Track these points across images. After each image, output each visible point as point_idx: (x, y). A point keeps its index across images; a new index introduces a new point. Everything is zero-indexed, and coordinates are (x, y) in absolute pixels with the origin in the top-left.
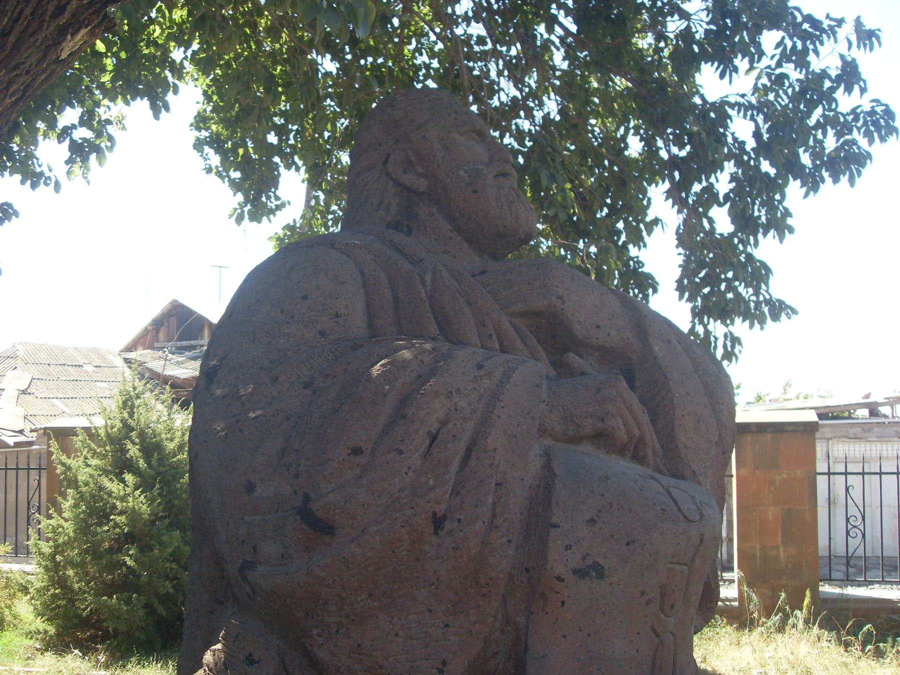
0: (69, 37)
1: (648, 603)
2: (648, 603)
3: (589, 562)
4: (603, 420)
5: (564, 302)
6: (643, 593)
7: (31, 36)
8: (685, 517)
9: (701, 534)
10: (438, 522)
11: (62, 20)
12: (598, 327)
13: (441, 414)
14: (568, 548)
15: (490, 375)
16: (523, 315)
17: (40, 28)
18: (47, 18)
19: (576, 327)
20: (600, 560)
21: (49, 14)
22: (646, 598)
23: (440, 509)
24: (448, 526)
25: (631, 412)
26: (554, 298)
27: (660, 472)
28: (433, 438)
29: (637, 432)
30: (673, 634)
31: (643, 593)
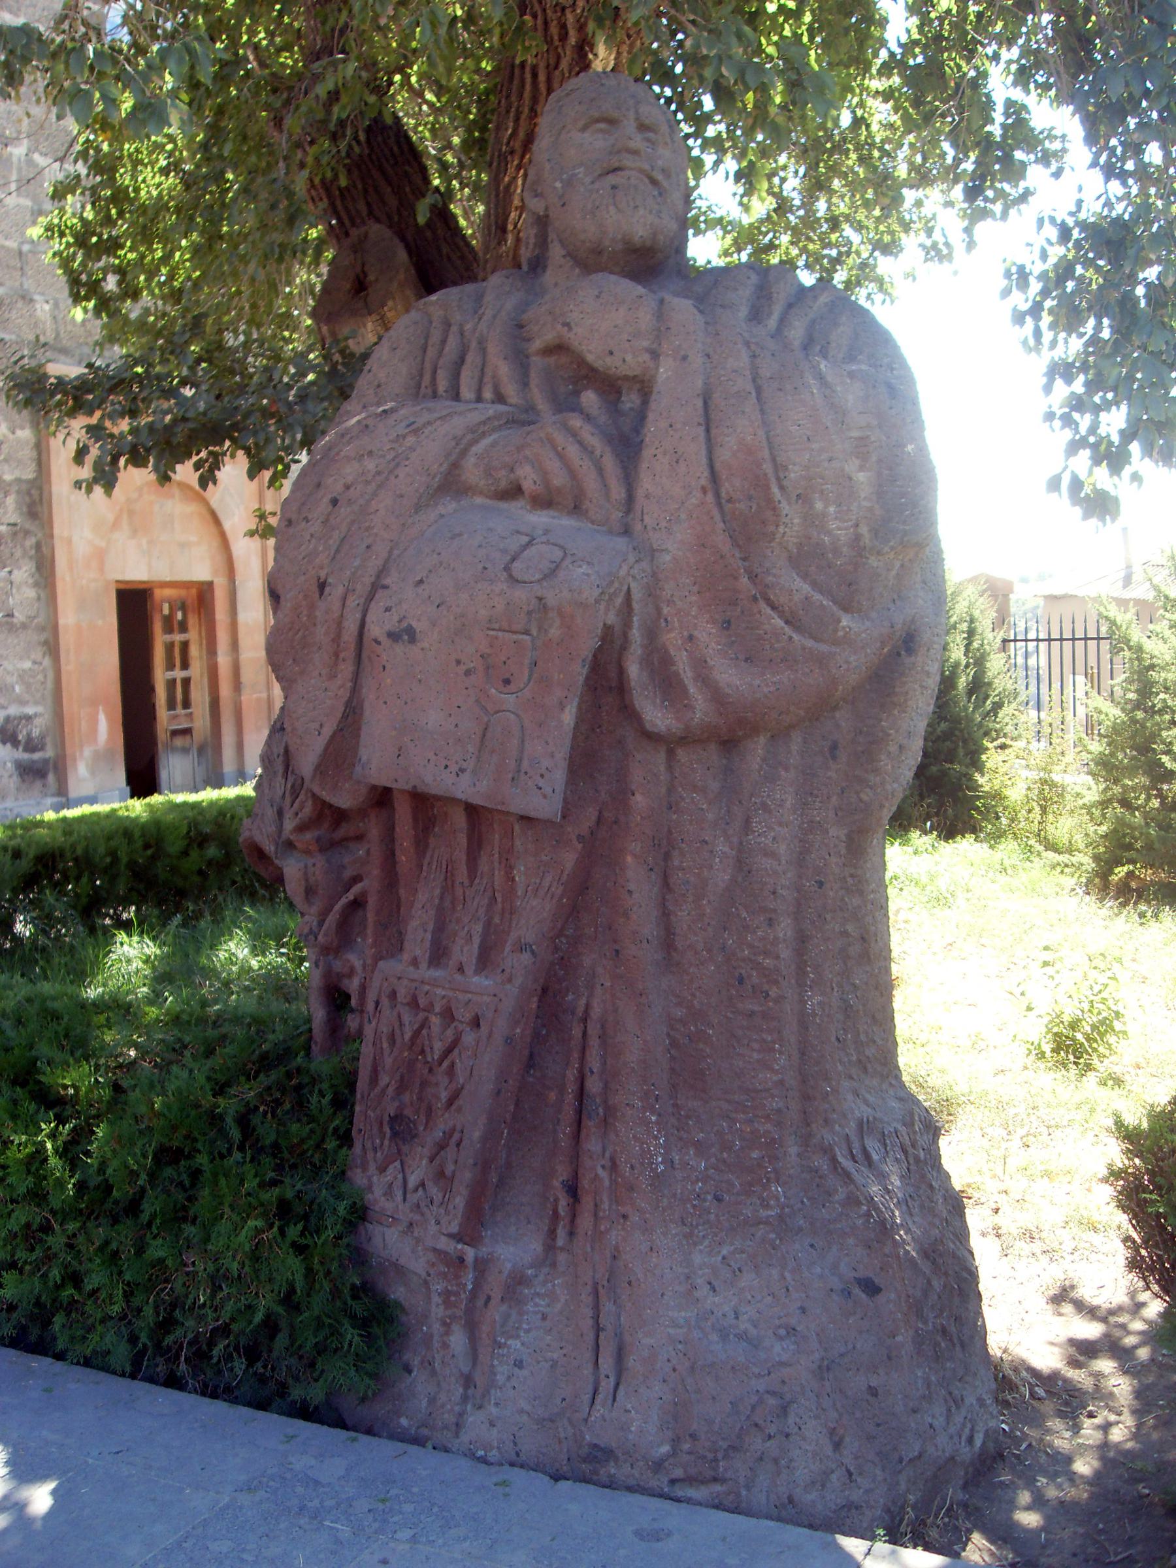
0: (591, 56)
1: (468, 673)
2: (468, 673)
3: (404, 625)
4: (512, 470)
5: (570, 329)
6: (458, 662)
7: (556, 67)
8: (511, 576)
9: (540, 599)
10: (322, 586)
11: (573, 40)
12: (611, 353)
13: (350, 479)
14: (388, 609)
15: (415, 432)
16: (549, 351)
17: (559, 58)
18: (557, 43)
19: (590, 358)
20: (414, 624)
21: (556, 38)
22: (463, 668)
23: (323, 574)
24: (327, 590)
25: (561, 456)
26: (559, 327)
27: (610, 532)
28: (335, 502)
29: (559, 479)
30: (518, 716)
31: (458, 662)
